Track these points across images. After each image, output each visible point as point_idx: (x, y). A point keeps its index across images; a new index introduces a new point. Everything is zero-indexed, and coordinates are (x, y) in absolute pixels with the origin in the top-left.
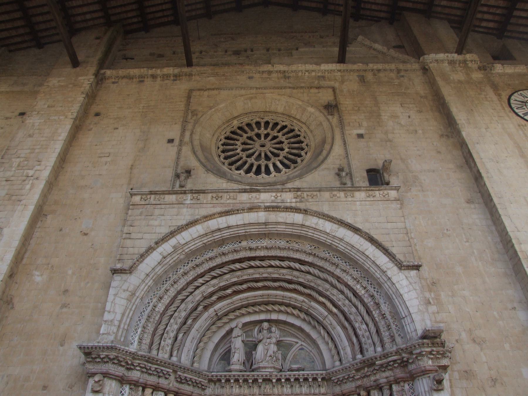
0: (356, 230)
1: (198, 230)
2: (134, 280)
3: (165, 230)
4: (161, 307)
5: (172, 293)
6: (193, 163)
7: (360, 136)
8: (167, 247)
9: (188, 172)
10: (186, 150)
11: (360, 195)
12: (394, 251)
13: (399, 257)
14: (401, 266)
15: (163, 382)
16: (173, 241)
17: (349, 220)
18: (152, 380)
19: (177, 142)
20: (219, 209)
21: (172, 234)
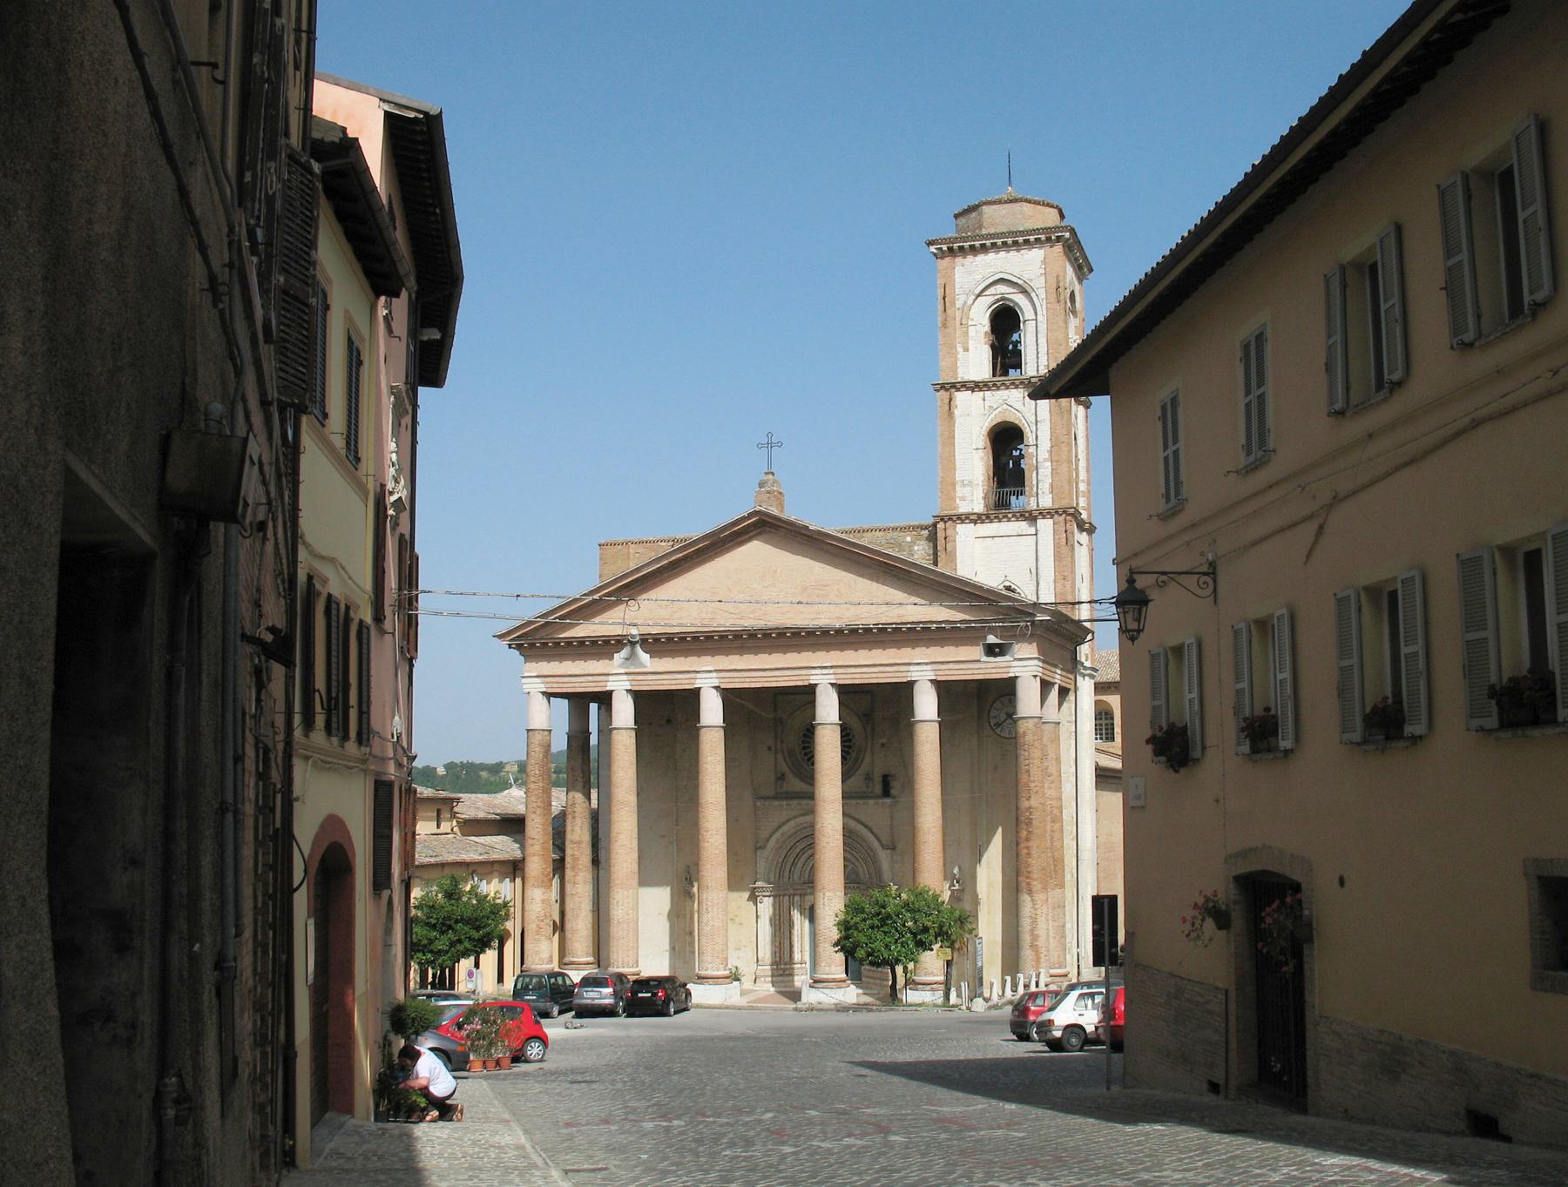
0: (866, 826)
1: (792, 824)
2: (766, 852)
3: (776, 824)
4: (781, 860)
5: (785, 852)
6: (785, 769)
7: (883, 745)
8: (778, 834)
9: (783, 775)
10: (780, 756)
11: (871, 802)
12: (882, 839)
13: (884, 843)
14: (883, 846)
15: (787, 892)
16: (780, 831)
17: (863, 820)
18: (781, 893)
19: (773, 748)
20: (801, 812)
21: (780, 827)
